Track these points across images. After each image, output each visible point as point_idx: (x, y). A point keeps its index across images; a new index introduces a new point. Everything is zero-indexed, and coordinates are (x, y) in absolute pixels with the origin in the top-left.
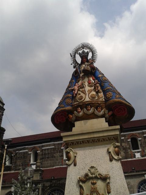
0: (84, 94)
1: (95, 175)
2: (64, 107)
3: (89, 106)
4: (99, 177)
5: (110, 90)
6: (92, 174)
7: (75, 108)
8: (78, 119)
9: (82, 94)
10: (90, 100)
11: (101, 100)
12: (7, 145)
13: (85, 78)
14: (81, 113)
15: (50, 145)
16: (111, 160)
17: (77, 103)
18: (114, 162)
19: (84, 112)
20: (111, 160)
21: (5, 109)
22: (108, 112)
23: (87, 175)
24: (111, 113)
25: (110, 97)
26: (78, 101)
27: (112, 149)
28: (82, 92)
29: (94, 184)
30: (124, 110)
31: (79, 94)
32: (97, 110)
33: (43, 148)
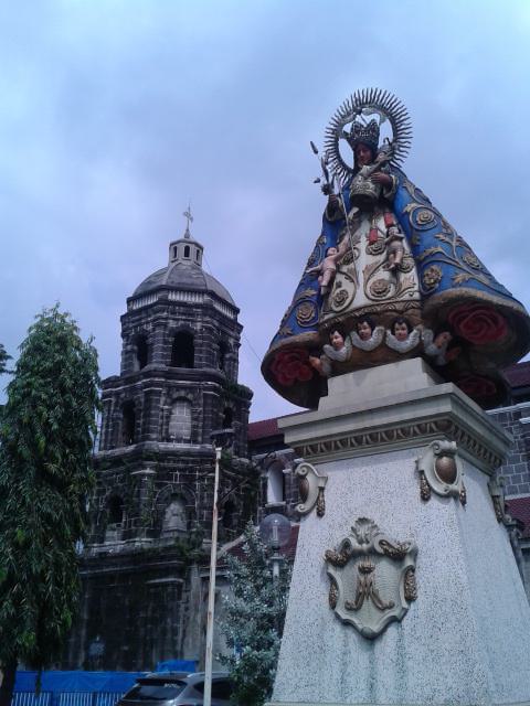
0: (353, 281)
1: (369, 545)
2: (291, 335)
3: (365, 323)
4: (381, 551)
5: (438, 258)
6: (361, 542)
7: (326, 334)
8: (339, 368)
9: (347, 286)
10: (370, 302)
11: (406, 297)
12: (220, 449)
13: (360, 222)
14: (344, 350)
16: (425, 498)
17: (331, 315)
18: (434, 501)
19: (354, 343)
20: (425, 498)
21: (242, 327)
22: (436, 336)
23: (346, 544)
24: (444, 338)
25: (435, 282)
26: (332, 311)
27: (427, 460)
28: (348, 278)
29: (365, 571)
30: (495, 321)
31: (339, 285)
32: (393, 333)
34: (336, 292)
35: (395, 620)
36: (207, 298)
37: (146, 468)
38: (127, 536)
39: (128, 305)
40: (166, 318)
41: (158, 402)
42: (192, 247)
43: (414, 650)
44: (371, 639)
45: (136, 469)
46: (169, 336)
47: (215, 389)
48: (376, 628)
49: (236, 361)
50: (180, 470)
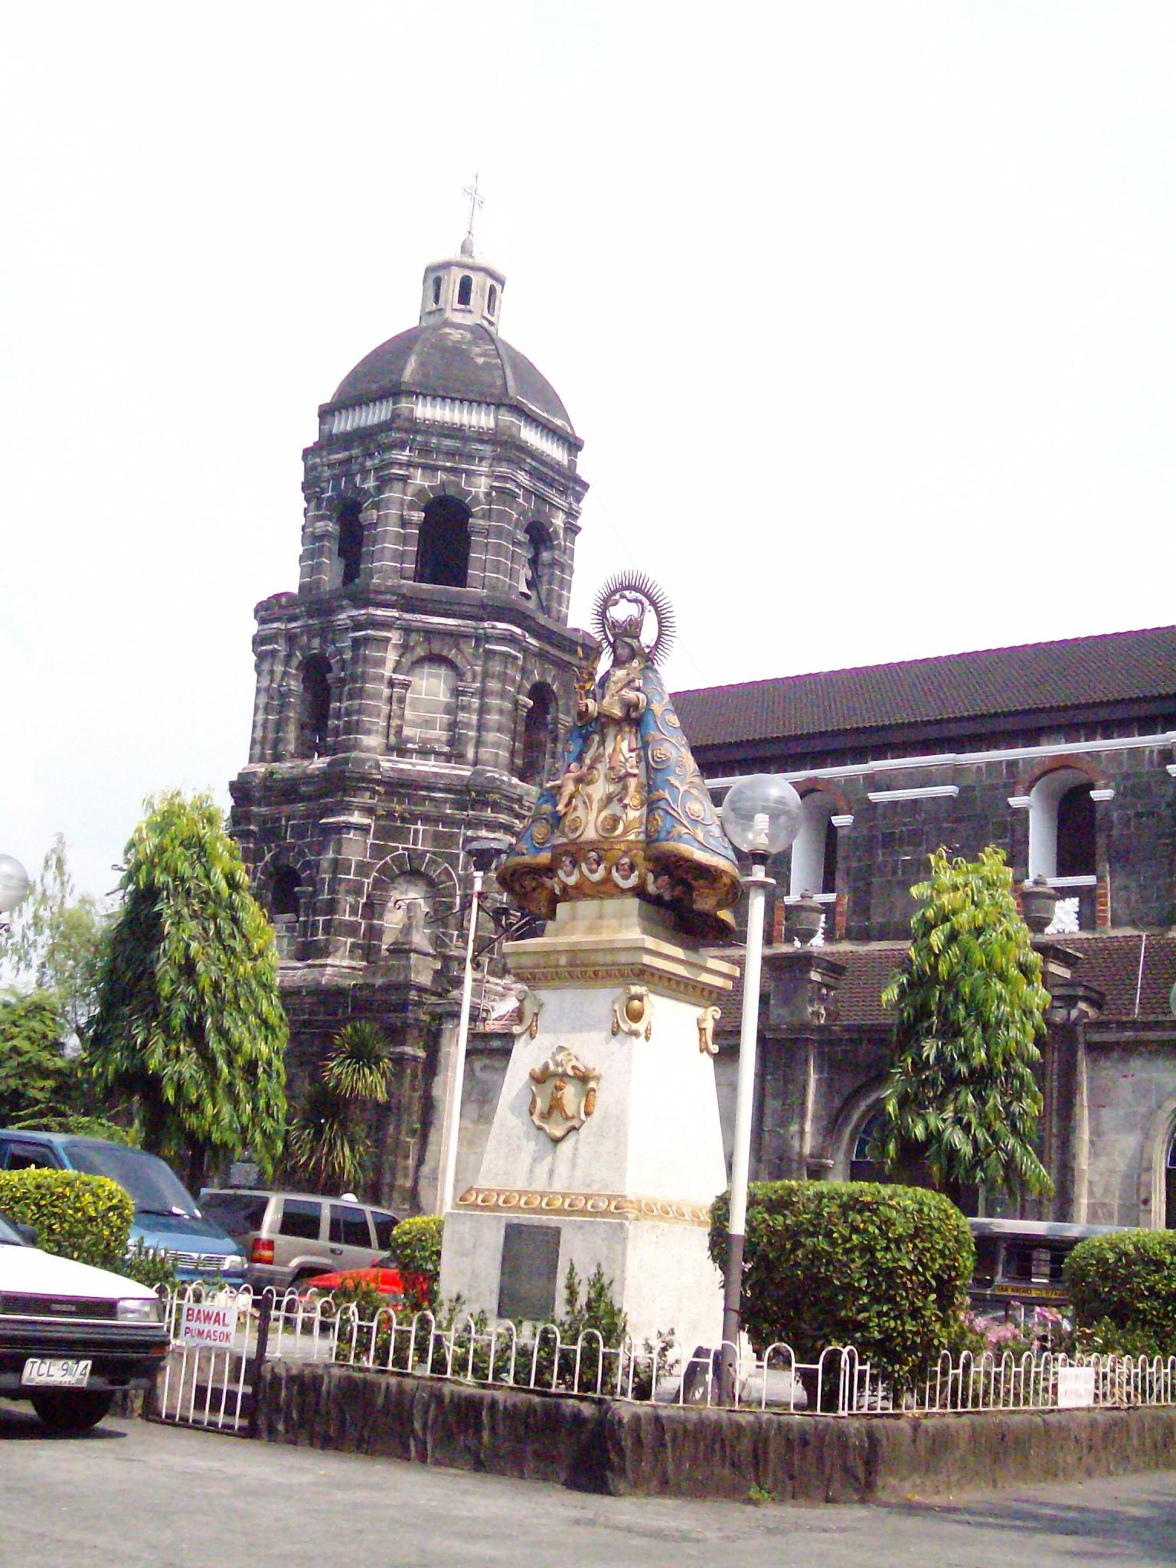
8: (568, 894)
12: (481, 874)
15: (925, 778)
16: (614, 1034)
18: (621, 1035)
20: (614, 1034)
21: (585, 486)
23: (546, 1067)
29: (558, 1088)
33: (874, 796)
34: (571, 816)
35: (574, 1128)
36: (507, 418)
37: (351, 815)
38: (307, 951)
39: (321, 423)
40: (409, 464)
41: (381, 663)
42: (477, 278)
43: (582, 1151)
44: (556, 1141)
45: (332, 812)
46: (412, 506)
47: (511, 639)
48: (558, 1132)
49: (566, 568)
50: (427, 819)
